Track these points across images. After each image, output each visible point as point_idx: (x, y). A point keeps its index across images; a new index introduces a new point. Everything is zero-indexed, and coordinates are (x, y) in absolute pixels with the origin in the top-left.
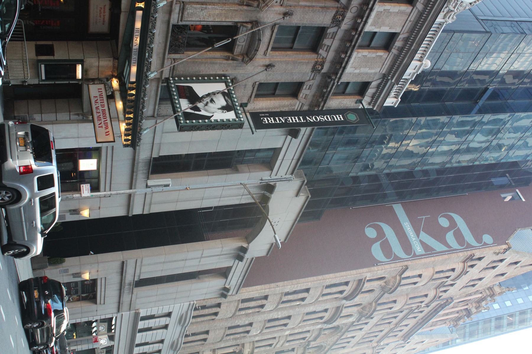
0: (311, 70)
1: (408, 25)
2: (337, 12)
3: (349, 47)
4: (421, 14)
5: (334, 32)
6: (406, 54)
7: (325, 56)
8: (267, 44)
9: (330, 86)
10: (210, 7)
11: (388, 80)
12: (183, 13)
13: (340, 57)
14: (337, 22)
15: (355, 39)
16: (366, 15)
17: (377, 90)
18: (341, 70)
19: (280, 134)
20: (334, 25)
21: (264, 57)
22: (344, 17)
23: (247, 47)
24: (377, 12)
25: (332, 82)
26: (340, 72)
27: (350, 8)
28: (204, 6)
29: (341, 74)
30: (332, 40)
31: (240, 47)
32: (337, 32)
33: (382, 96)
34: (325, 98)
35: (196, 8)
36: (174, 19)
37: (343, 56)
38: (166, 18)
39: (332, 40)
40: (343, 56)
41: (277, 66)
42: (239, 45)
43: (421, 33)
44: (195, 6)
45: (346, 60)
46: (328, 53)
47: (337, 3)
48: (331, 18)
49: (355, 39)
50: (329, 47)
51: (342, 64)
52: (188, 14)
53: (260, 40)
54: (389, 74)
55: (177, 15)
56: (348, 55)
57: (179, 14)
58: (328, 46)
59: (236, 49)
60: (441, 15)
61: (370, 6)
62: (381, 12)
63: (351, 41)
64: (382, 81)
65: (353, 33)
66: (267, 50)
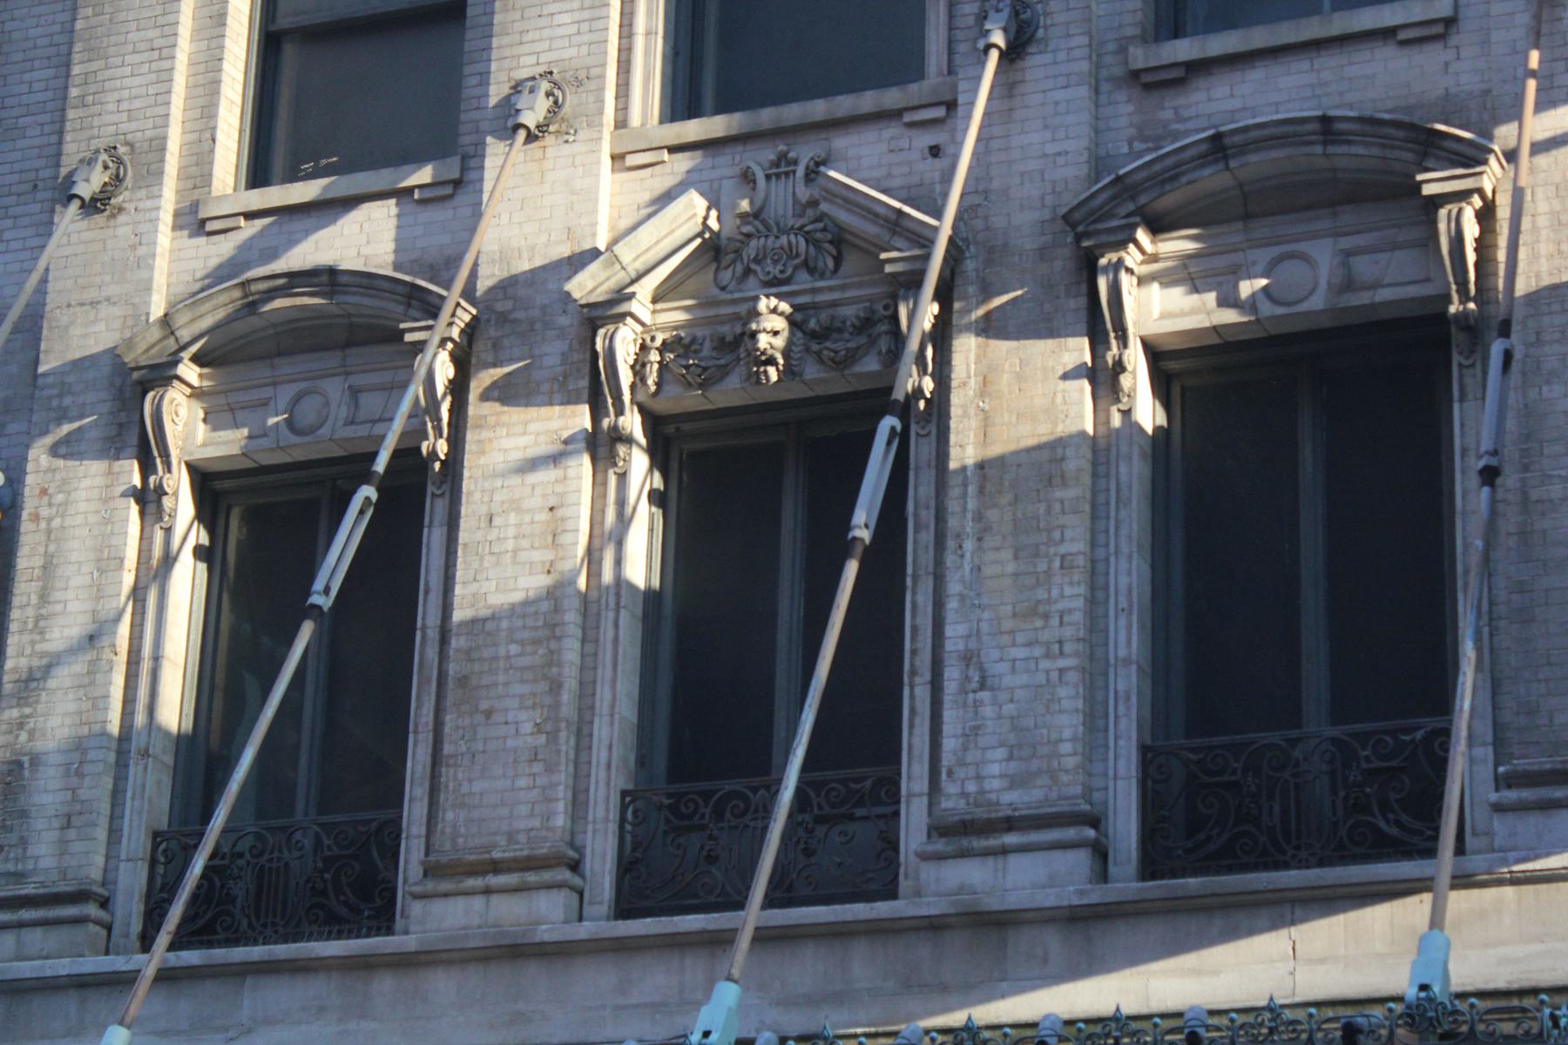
8: (1329, 64)
10: (955, 631)
12: (1010, 824)
21: (1464, 38)
23: (1348, 217)
28: (952, 675)
31: (1363, 267)
35: (972, 734)
36: (1051, 882)
38: (1052, 941)
44: (949, 744)
52: (1015, 782)
53: (1218, 147)
55: (1013, 859)
57: (1004, 851)
66: (1386, 34)
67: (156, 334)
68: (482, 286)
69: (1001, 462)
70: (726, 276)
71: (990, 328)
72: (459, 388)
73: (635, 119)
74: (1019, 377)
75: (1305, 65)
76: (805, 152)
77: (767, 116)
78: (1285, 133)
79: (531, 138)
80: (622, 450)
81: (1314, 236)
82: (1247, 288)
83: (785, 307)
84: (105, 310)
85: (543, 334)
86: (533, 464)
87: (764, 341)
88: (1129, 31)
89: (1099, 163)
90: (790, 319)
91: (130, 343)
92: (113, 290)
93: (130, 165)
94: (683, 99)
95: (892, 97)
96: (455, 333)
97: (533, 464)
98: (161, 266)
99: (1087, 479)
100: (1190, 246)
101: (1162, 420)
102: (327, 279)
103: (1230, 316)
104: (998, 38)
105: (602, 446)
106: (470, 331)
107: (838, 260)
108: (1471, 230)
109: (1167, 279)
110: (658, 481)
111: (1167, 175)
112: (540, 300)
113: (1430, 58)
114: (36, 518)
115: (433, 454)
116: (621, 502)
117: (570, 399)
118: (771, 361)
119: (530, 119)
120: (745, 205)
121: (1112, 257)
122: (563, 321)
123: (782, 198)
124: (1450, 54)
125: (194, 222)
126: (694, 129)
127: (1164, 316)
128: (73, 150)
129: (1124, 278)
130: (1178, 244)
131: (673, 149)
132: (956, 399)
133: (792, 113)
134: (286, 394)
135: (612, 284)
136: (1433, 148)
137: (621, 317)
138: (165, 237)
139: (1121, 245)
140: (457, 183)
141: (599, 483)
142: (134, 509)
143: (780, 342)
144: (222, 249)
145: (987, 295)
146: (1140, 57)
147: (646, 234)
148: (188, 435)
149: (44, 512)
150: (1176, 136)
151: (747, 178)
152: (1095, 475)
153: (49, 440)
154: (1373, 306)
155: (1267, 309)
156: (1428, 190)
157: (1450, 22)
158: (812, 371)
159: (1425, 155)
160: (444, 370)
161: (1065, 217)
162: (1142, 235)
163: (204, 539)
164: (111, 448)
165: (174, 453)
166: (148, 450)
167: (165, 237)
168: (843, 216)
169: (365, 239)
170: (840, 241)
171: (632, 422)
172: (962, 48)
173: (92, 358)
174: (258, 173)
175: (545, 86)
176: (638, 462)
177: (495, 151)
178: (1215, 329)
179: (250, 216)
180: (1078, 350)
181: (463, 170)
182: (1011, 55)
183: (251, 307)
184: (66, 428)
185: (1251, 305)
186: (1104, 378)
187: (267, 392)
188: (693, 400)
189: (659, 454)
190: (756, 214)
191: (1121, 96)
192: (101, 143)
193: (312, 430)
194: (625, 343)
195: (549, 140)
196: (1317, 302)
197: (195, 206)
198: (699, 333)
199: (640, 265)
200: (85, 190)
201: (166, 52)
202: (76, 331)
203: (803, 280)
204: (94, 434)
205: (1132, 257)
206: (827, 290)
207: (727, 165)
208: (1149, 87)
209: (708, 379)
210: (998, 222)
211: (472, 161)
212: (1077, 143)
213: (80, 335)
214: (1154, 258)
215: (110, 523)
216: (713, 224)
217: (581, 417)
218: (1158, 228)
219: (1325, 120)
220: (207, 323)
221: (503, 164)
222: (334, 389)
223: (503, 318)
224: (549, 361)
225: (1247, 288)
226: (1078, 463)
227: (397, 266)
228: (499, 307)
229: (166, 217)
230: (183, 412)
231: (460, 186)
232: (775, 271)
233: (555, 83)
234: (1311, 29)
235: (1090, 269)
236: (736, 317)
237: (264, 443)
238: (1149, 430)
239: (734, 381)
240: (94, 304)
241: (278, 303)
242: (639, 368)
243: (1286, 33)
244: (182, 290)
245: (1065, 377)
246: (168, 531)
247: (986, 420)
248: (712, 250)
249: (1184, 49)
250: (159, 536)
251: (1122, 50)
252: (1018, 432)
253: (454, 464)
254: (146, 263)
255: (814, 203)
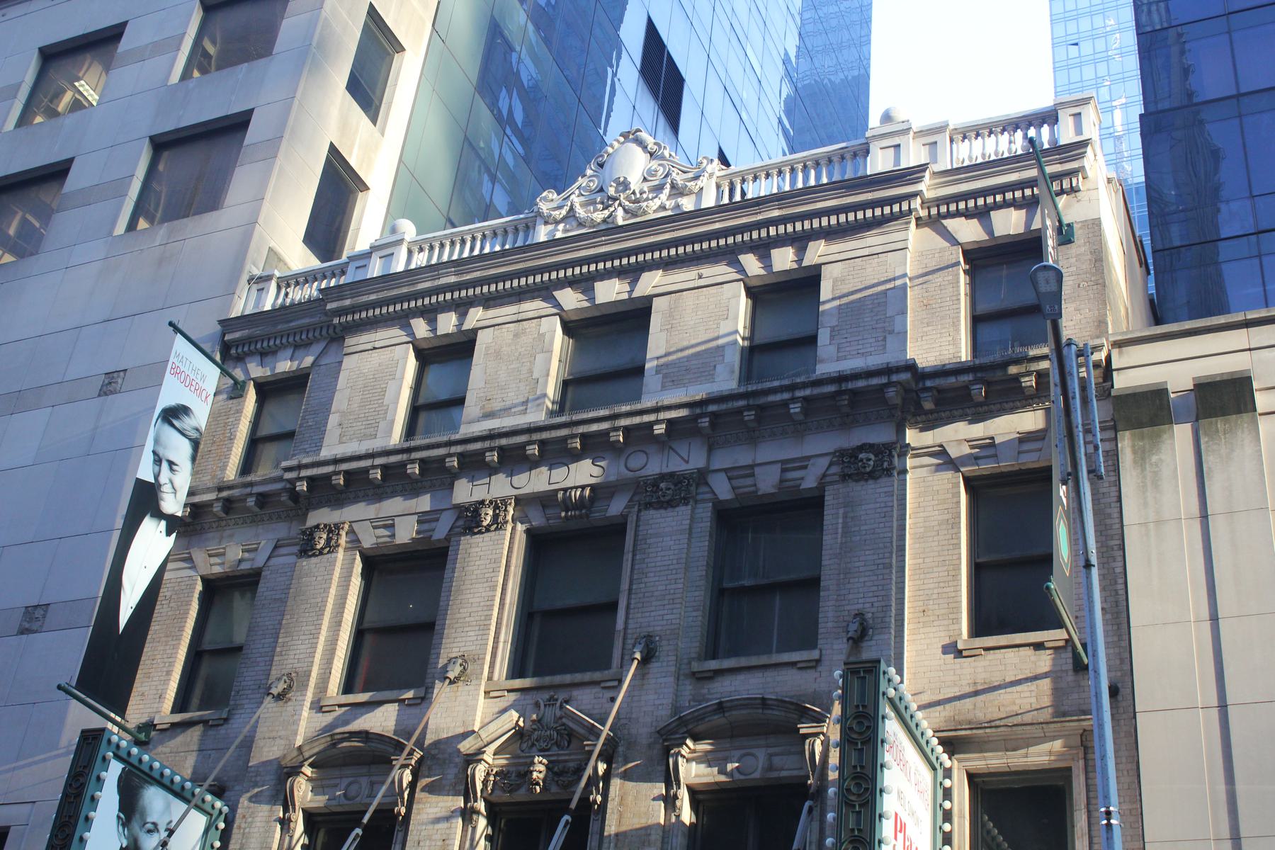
0: (884, 480)
1: (720, 271)
2: (649, 505)
3: (761, 408)
4: (668, 265)
5: (730, 479)
6: (802, 217)
7: (825, 462)
8: (770, 675)
9: (952, 380)
11: (939, 201)
13: (805, 412)
14: (675, 491)
15: (723, 407)
16: (637, 420)
17: (997, 206)
18: (851, 385)
19: (1249, 450)
20: (706, 489)
22: (662, 477)
24: (664, 388)
25: (929, 383)
26: (861, 383)
27: (630, 474)
29: (869, 374)
30: (757, 470)
32: (726, 470)
33: (1013, 177)
34: (1013, 370)
37: (795, 408)
39: (757, 470)
40: (795, 408)
41: (854, 608)
42: (770, 768)
43: (717, 226)
45: (808, 392)
46: (808, 458)
47: (629, 519)
48: (670, 509)
49: (723, 407)
50: (786, 466)
51: (834, 396)
53: (721, 707)
54: (902, 215)
56: (786, 396)
58: (784, 471)
59: (784, 774)
60: (688, 204)
61: (605, 426)
62: (665, 376)
63: (739, 412)
64: (949, 215)
65: (705, 422)
66: (793, 664)
67: (295, 753)
68: (427, 742)
69: (625, 833)
70: (524, 746)
71: (626, 776)
72: (413, 785)
73: (496, 677)
74: (636, 798)
75: (760, 675)
76: (561, 696)
77: (547, 680)
78: (747, 703)
79: (452, 682)
80: (475, 817)
81: (759, 747)
82: (730, 767)
83: (545, 761)
84: (278, 741)
85: (446, 764)
86: (437, 820)
87: (535, 775)
88: (693, 655)
89: (676, 709)
90: (547, 766)
91: (284, 757)
92: (282, 733)
93: (295, 682)
94: (517, 670)
95: (597, 676)
96: (413, 762)
97: (437, 820)
98: (303, 724)
99: (659, 844)
100: (709, 747)
101: (694, 820)
102: (365, 735)
103: (723, 778)
104: (638, 656)
105: (467, 815)
106: (420, 761)
107: (569, 743)
108: (818, 748)
109: (699, 760)
110: (490, 831)
111: (699, 717)
112: (449, 750)
113: (810, 675)
114: (239, 827)
115: (399, 813)
116: (472, 839)
117: (456, 794)
118: (538, 784)
119: (451, 675)
120: (534, 717)
121: (676, 750)
122: (457, 760)
123: (550, 714)
124: (817, 675)
125: (318, 707)
126: (518, 683)
127: (696, 776)
128: (274, 673)
129: (680, 759)
130: (704, 746)
131: (509, 691)
132: (609, 806)
133: (558, 679)
134: (345, 782)
135: (477, 746)
136: (806, 715)
137: (479, 761)
138: (305, 713)
139: (680, 745)
140: (423, 699)
141: (464, 830)
142: (279, 827)
143: (541, 776)
144: (327, 719)
145: (626, 762)
146: (696, 666)
147: (492, 727)
148: (304, 797)
149: (243, 825)
150: (708, 700)
151: (537, 705)
152: (663, 842)
153: (248, 795)
154: (779, 778)
155: (737, 776)
156: (802, 731)
157: (818, 661)
158: (554, 789)
159: (802, 717)
160: (407, 777)
161: (658, 732)
162: (689, 742)
163: (307, 842)
164: (272, 800)
165: (297, 804)
166: (288, 804)
167: (305, 713)
168: (571, 724)
169: (383, 720)
170: (571, 735)
171: (481, 806)
172: (626, 657)
173: (270, 761)
174: (348, 688)
175: (460, 661)
176: (482, 823)
177: (438, 684)
178: (716, 783)
179: (340, 706)
180: (660, 788)
181: (426, 693)
182: (645, 661)
183: (334, 745)
184: (256, 790)
185: (730, 774)
186: (670, 801)
187: (337, 781)
188: (506, 797)
189: (492, 818)
190: (539, 721)
191: (687, 682)
192: (285, 672)
193: (353, 798)
194: (480, 772)
195: (460, 683)
196: (757, 775)
197: (319, 700)
198: (511, 769)
199: (488, 739)
200: (275, 691)
201: (315, 636)
202: (266, 749)
203: (555, 750)
204: (267, 794)
205: (684, 751)
206: (564, 755)
207: (530, 699)
208: (699, 679)
209: (512, 789)
210: (634, 731)
211: (429, 689)
212: (667, 701)
213: (268, 750)
214: (694, 751)
215: (268, 833)
216: (521, 723)
217: (460, 802)
218: (696, 739)
219: (763, 699)
220: (316, 750)
221: (442, 692)
222: (364, 781)
223: (434, 757)
224: (450, 777)
225: (730, 767)
226: (656, 837)
227: (395, 732)
228: (433, 752)
229: (307, 704)
230: (303, 787)
231: (424, 700)
232: (544, 745)
233: (465, 660)
234: (764, 660)
235: (666, 753)
236: (525, 764)
237: (334, 803)
238: (688, 823)
239: (523, 791)
240: (274, 738)
241: (345, 744)
242: (485, 783)
243: (754, 661)
244: (310, 735)
245: (654, 799)
246: (291, 837)
247: (621, 815)
248: (519, 734)
249: (713, 665)
250: (287, 839)
251: (689, 663)
252: (633, 822)
253: (407, 817)
254: (297, 723)
255: (561, 718)
